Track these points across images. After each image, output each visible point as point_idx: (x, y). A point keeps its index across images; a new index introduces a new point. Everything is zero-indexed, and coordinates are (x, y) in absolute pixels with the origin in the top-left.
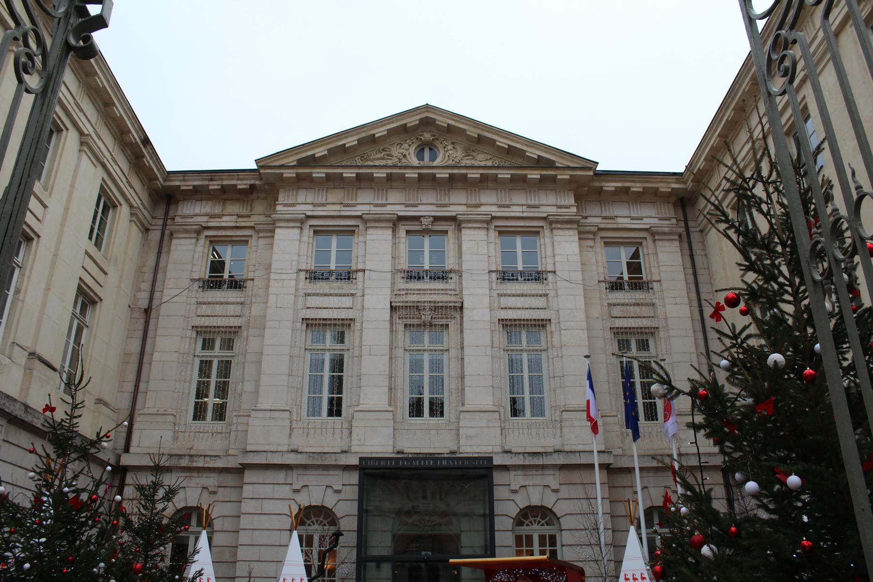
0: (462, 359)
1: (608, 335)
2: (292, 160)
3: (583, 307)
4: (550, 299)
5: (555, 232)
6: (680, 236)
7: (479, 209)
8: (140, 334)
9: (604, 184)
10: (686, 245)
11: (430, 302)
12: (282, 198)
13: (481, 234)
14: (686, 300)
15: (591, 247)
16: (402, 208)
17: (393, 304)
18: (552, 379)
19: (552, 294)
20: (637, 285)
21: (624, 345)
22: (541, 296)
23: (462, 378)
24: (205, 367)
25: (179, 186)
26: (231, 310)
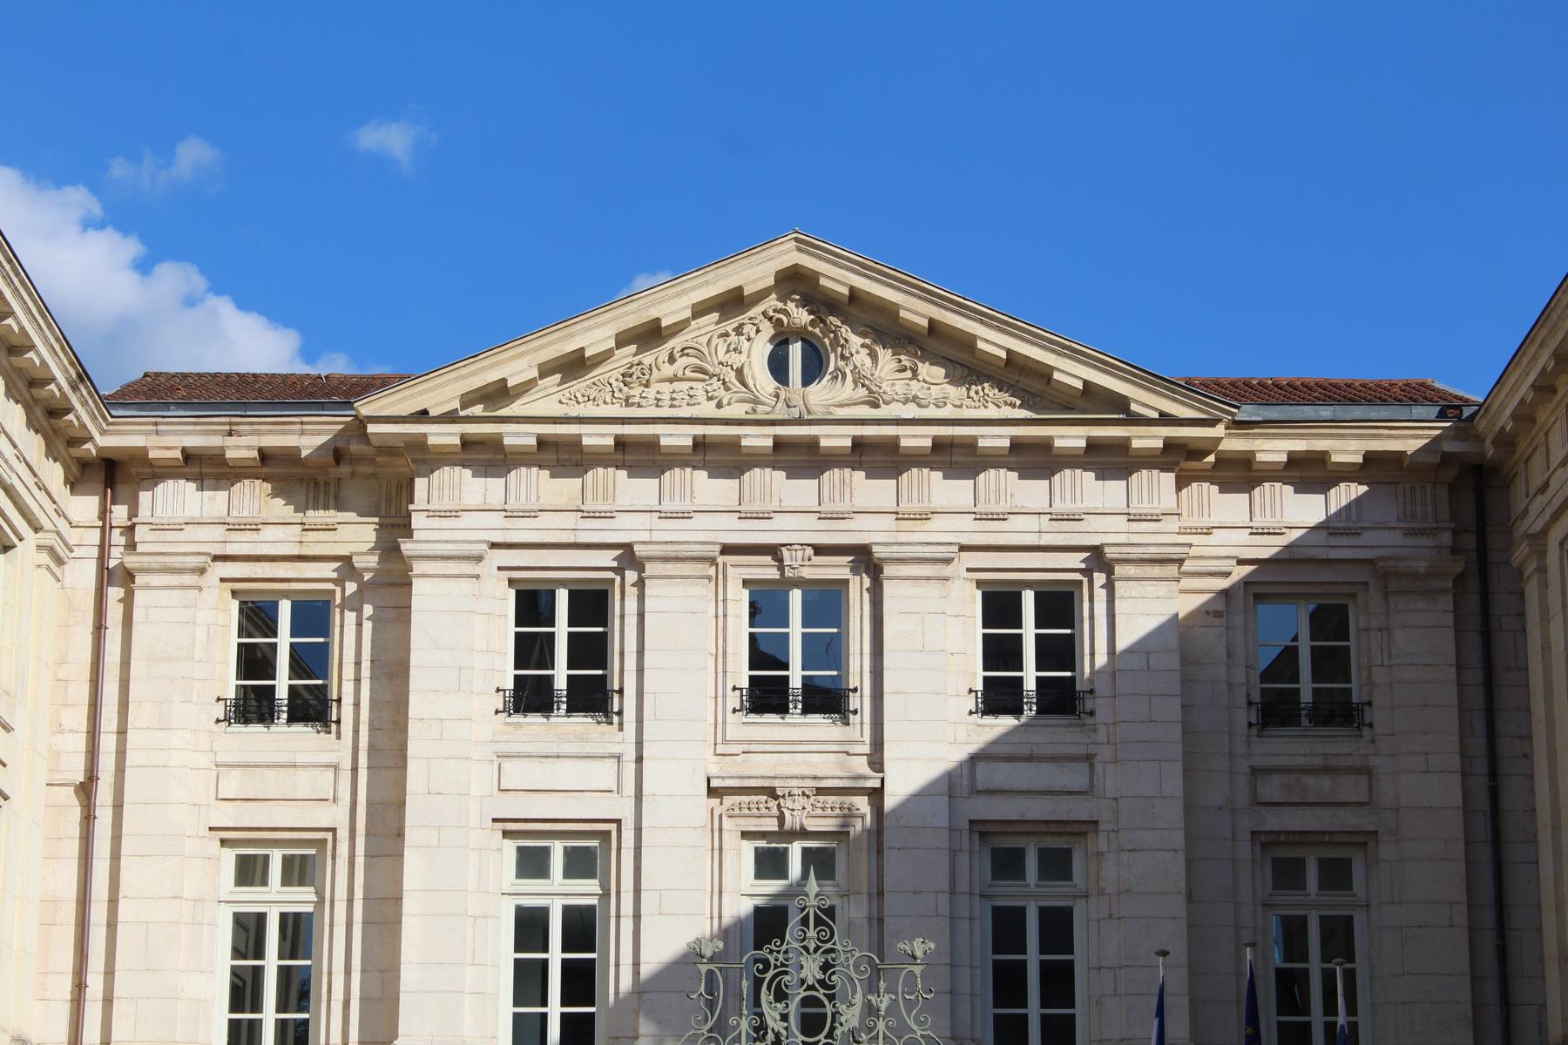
0: (881, 920)
3: (1179, 792)
4: (1099, 768)
7: (928, 525)
8: (73, 847)
14: (1455, 762)
16: (731, 521)
17: (715, 783)
19: (1104, 753)
20: (1340, 712)
21: (1288, 874)
22: (1075, 759)
24: (249, 932)
25: (145, 450)
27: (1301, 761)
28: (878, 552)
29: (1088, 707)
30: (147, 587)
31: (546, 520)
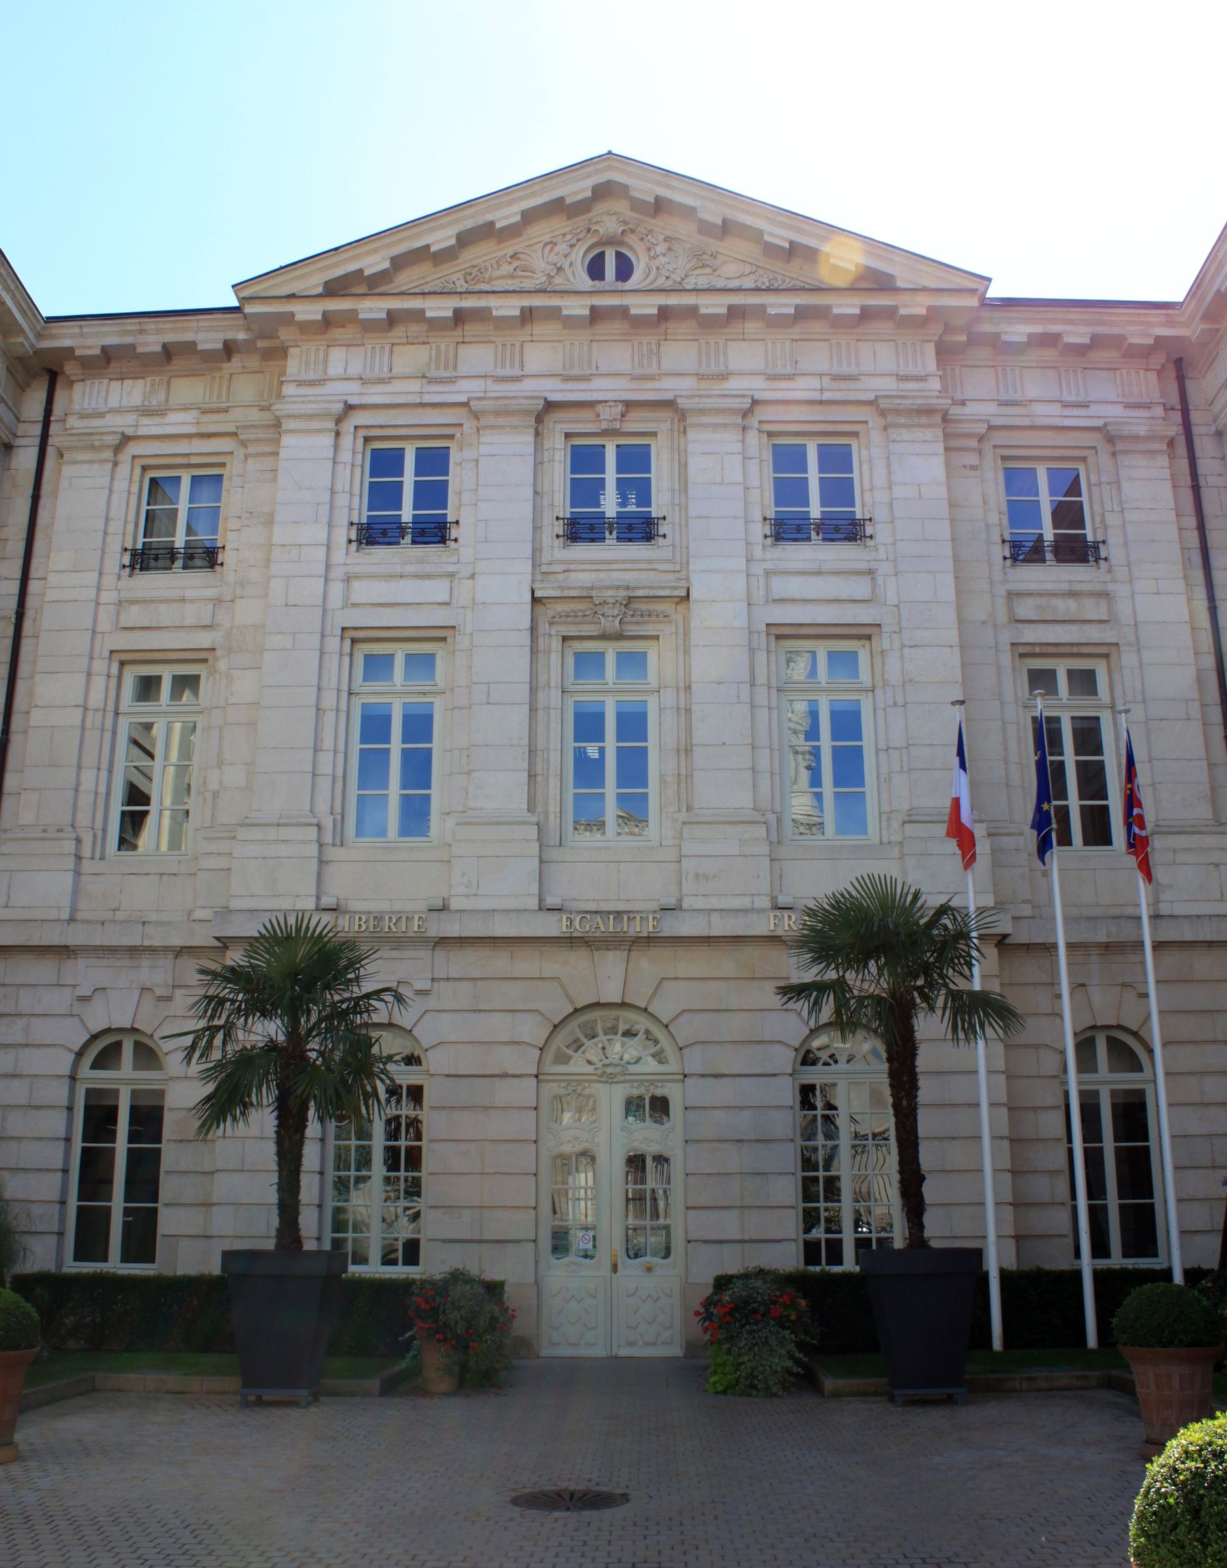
1: (1006, 658)
2: (314, 282)
4: (880, 580)
5: (894, 434)
6: (1171, 443)
9: (1003, 327)
10: (1184, 464)
11: (618, 588)
12: (293, 366)
13: (729, 440)
15: (973, 468)
17: (538, 594)
18: (882, 755)
19: (885, 568)
20: (1076, 550)
22: (859, 573)
23: (688, 751)
26: (191, 614)
27: (1050, 586)
28: (683, 403)
29: (868, 534)
30: (74, 462)
31: (398, 386)
